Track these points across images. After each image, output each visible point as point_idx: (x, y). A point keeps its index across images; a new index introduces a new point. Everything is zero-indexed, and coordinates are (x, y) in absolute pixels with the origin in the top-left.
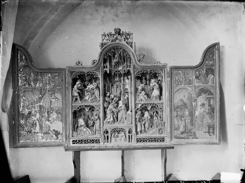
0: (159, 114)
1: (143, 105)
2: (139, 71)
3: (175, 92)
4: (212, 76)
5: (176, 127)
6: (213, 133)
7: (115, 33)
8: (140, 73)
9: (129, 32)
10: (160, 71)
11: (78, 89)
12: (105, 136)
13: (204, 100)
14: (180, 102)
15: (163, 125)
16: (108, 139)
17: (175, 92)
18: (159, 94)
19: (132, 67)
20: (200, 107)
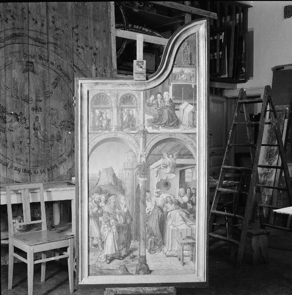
3: (92, 150)
4: (191, 107)
5: (95, 242)
6: (193, 259)
13: (168, 170)
14: (104, 174)
17: (92, 150)
20: (158, 190)
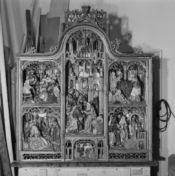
0: (140, 119)
1: (118, 109)
2: (114, 63)
7: (82, 11)
8: (116, 65)
9: (102, 10)
10: (142, 63)
11: (30, 85)
12: (66, 150)
15: (145, 136)
16: (70, 153)
18: (140, 94)
19: (104, 56)
